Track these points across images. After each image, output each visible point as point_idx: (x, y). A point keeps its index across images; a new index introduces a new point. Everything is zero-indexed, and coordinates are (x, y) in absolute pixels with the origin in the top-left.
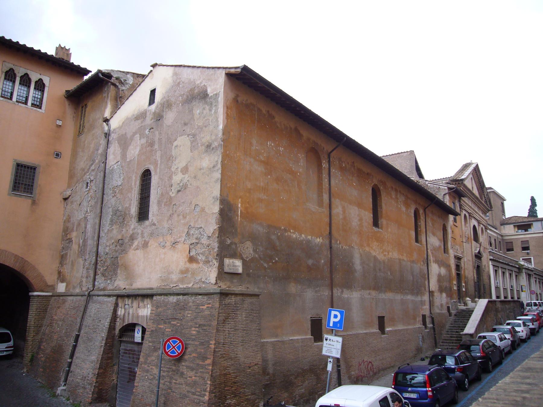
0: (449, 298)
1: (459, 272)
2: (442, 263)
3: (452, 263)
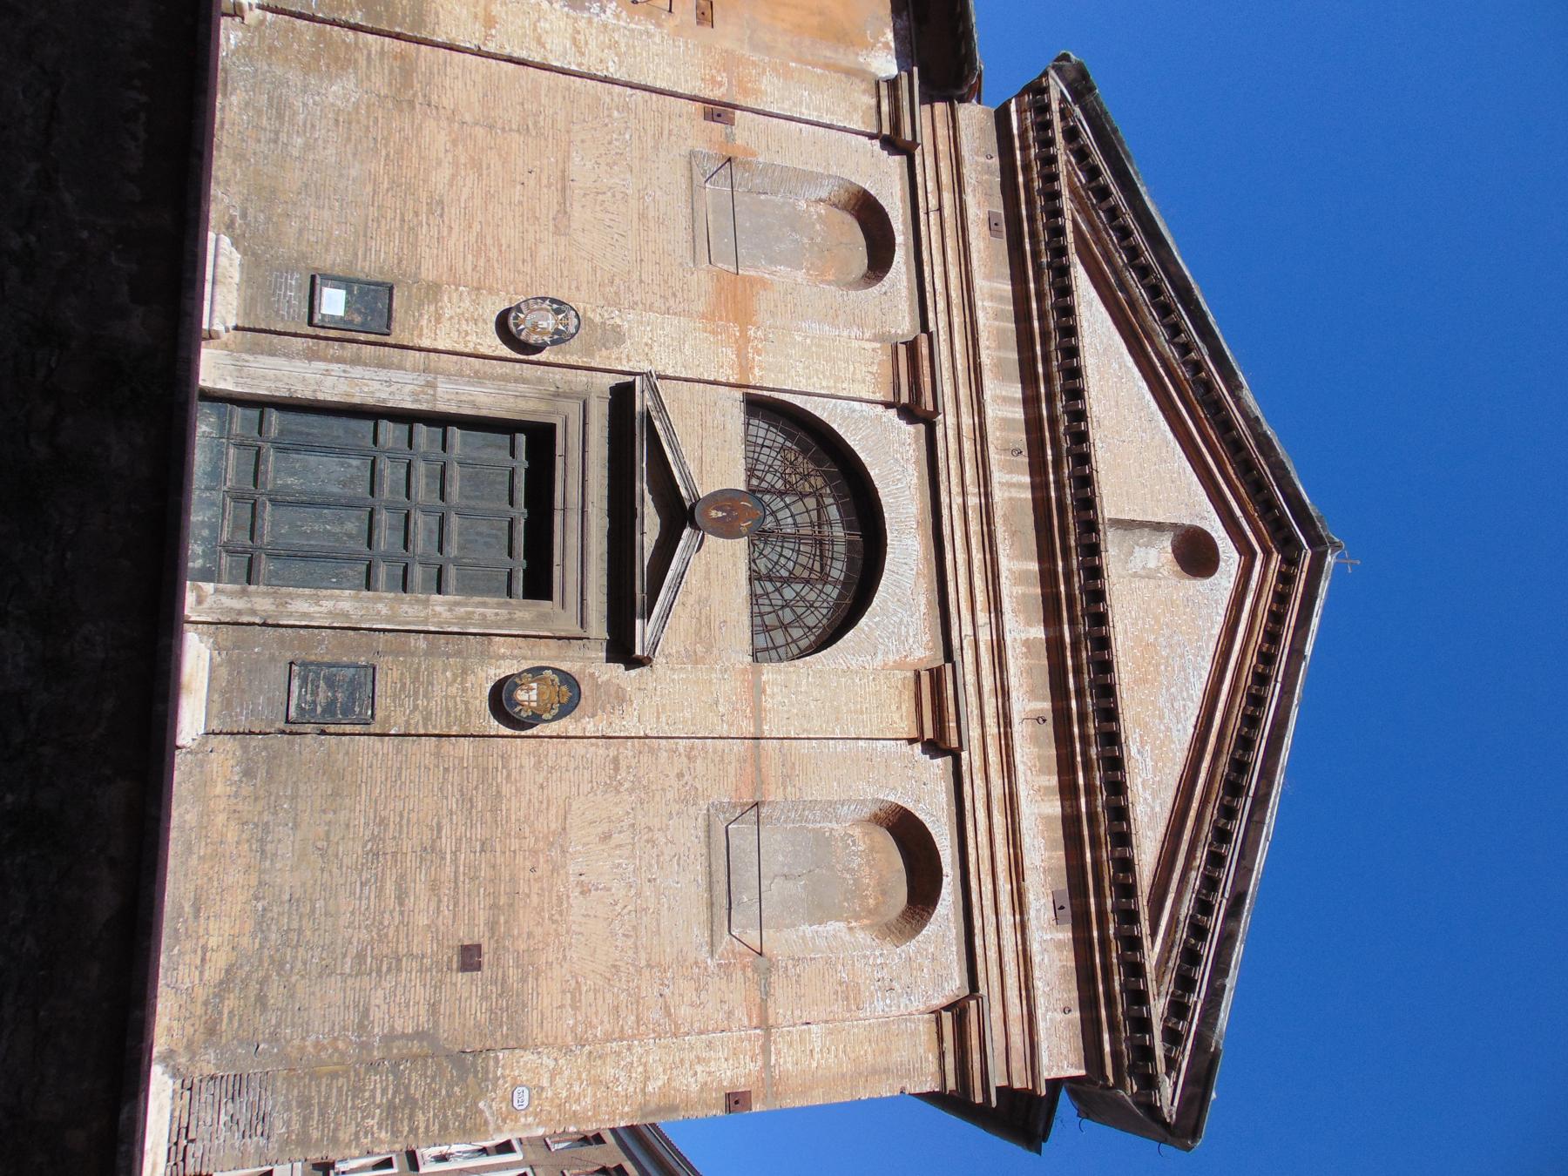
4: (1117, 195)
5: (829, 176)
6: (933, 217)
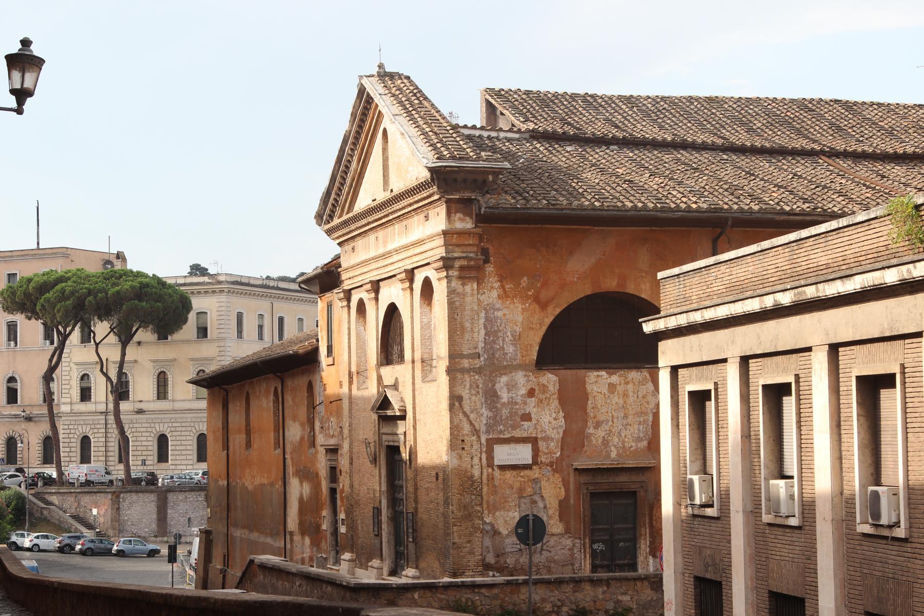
0: (315, 549)
1: (334, 485)
2: (307, 474)
3: (322, 465)
4: (333, 196)
5: (356, 328)
6: (356, 280)
